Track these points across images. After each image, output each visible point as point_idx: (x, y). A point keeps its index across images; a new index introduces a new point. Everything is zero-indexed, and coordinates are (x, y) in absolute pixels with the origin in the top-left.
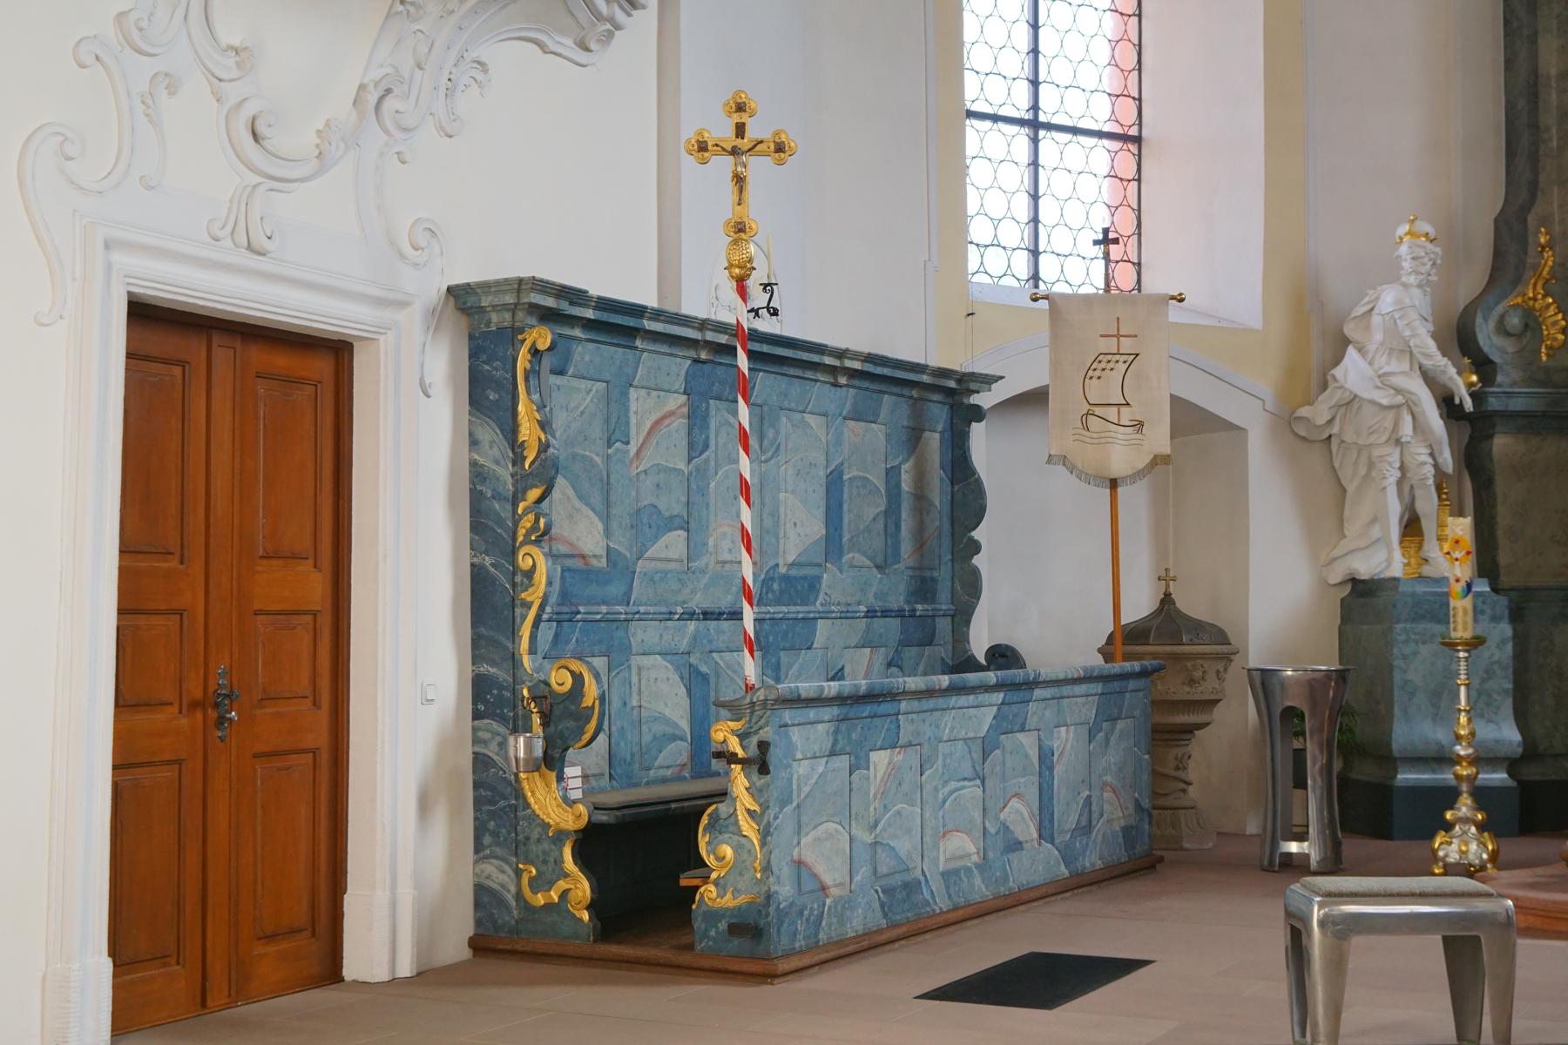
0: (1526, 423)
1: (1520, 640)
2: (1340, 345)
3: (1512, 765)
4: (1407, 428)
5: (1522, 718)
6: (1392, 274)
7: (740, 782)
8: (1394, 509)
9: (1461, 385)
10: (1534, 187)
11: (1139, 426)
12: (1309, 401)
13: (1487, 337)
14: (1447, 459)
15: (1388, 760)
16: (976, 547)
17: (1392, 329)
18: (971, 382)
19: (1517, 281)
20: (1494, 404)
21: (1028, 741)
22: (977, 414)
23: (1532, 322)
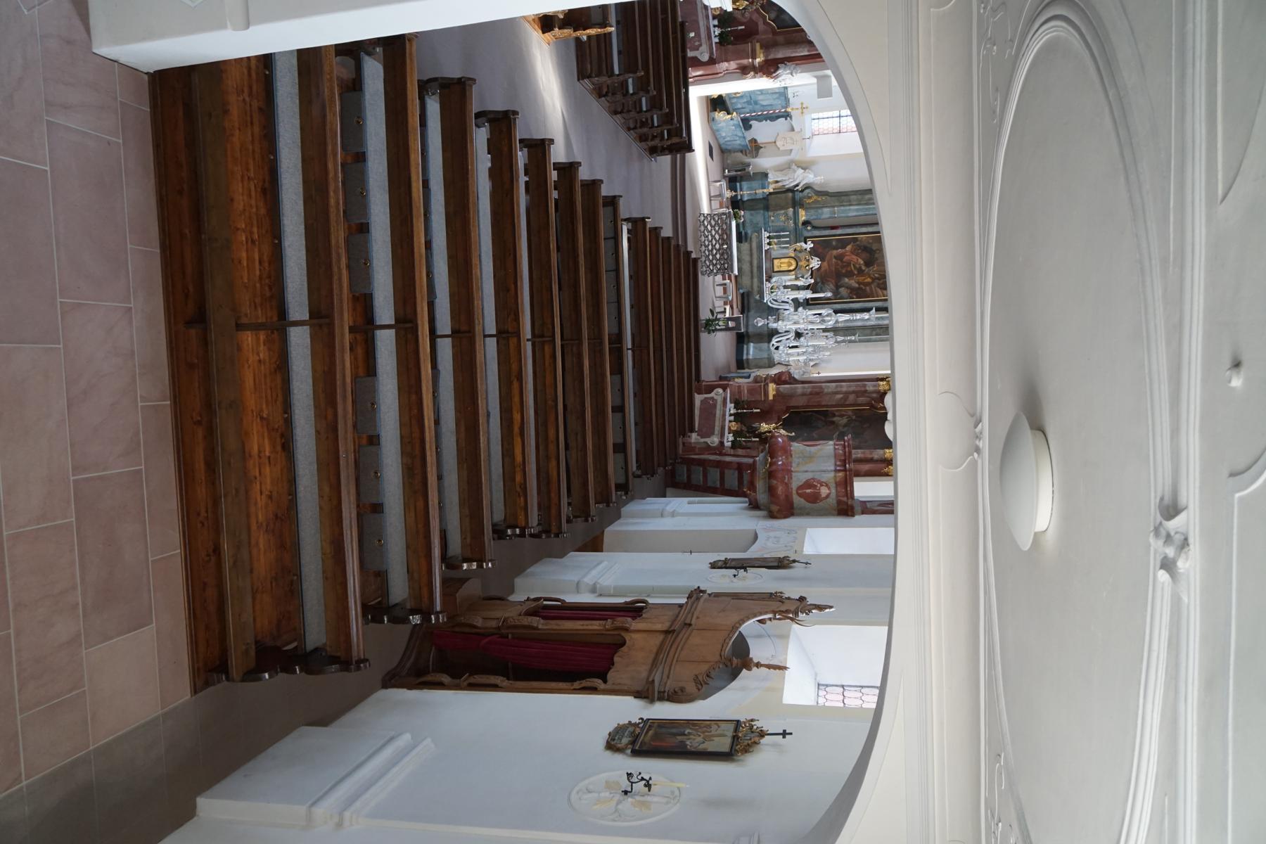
0: (794, 198)
1: (760, 199)
2: (804, 169)
3: (741, 199)
4: (791, 180)
5: (747, 200)
6: (815, 176)
7: (730, 116)
8: (779, 179)
9: (799, 188)
10: (831, 196)
11: (784, 145)
12: (796, 165)
13: (807, 191)
14: (787, 187)
15: (740, 182)
16: (766, 120)
17: (807, 176)
18: (791, 118)
19: (816, 195)
20: (796, 193)
21: (737, 138)
22: (786, 119)
23: (810, 198)
